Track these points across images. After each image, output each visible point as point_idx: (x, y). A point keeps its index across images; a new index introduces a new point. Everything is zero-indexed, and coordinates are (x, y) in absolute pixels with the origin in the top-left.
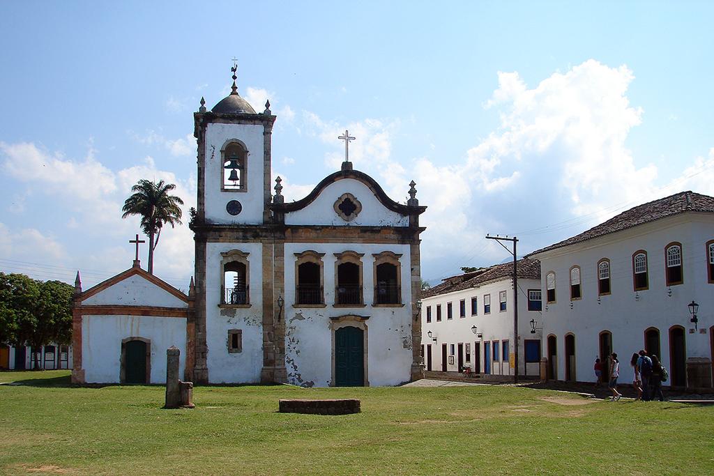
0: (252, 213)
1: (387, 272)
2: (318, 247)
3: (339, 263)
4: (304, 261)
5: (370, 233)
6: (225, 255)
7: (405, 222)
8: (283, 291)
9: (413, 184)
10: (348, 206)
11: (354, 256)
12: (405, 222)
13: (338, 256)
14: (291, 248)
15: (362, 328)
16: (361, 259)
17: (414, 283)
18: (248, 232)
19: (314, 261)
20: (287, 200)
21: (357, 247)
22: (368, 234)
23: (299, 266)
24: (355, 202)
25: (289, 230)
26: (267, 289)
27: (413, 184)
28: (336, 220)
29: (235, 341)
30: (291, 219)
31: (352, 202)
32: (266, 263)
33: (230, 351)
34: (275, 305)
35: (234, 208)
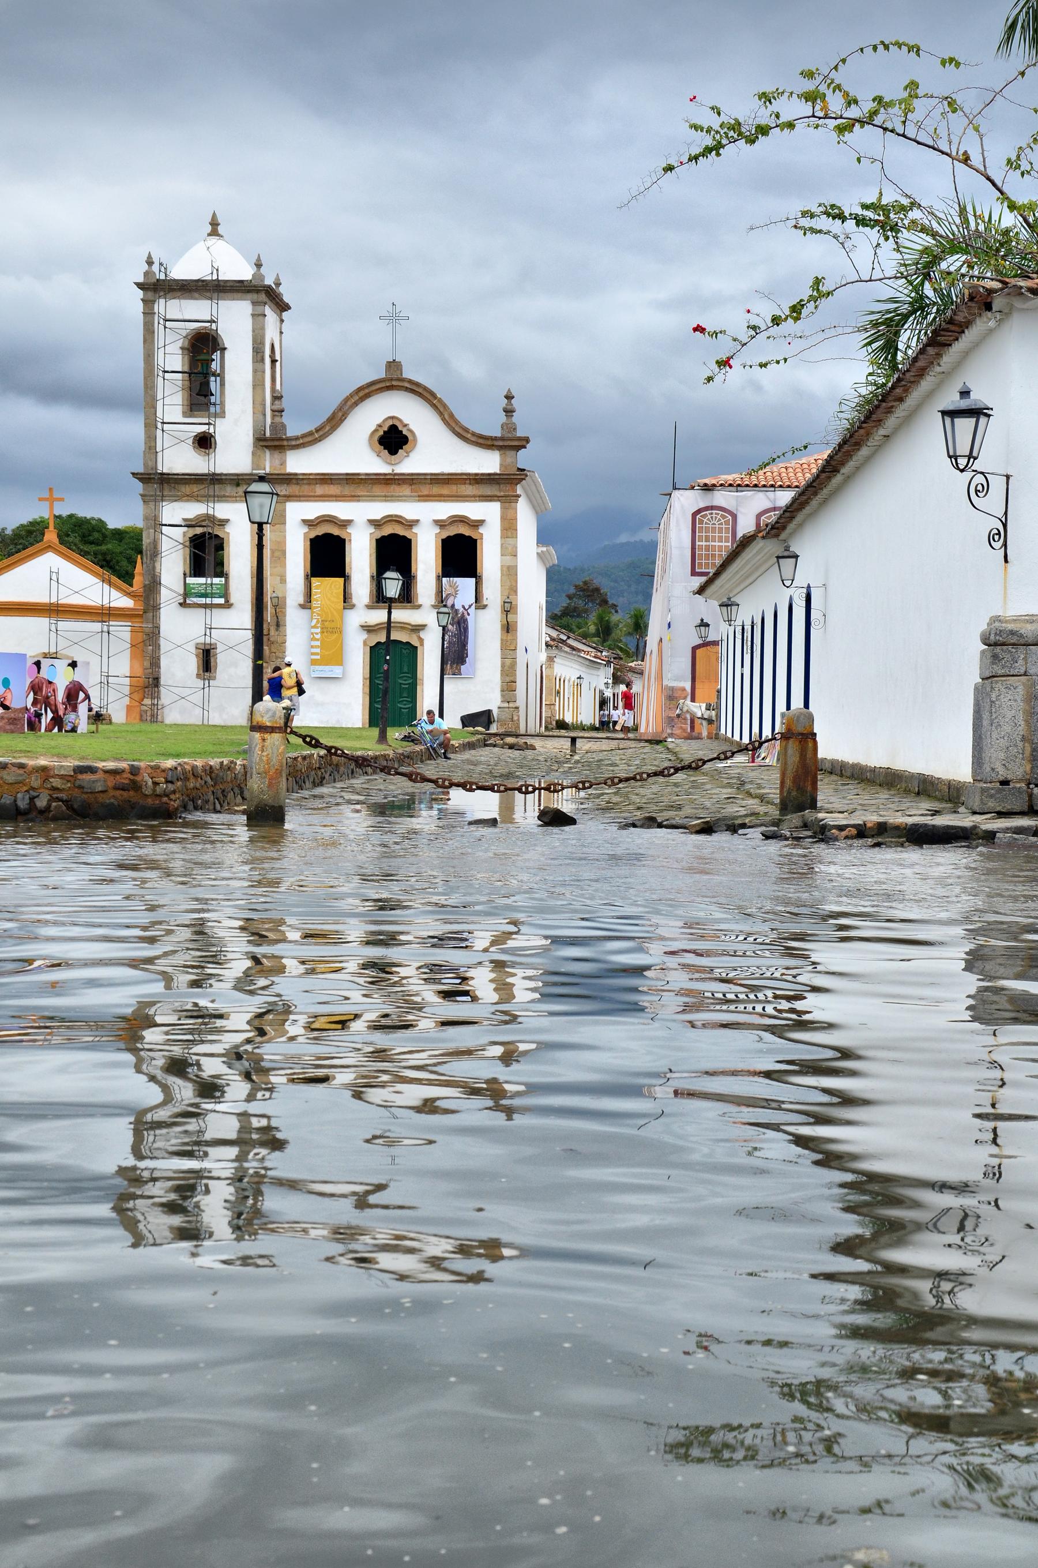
2: (340, 510)
3: (379, 534)
4: (320, 531)
8: (283, 580)
9: (509, 397)
11: (402, 523)
12: (489, 463)
13: (375, 523)
15: (415, 642)
16: (415, 530)
17: (505, 569)
19: (335, 531)
20: (290, 433)
21: (407, 510)
22: (425, 490)
23: (311, 540)
24: (405, 432)
25: (294, 481)
27: (509, 397)
28: (374, 463)
29: (207, 659)
30: (298, 463)
31: (401, 432)
33: (198, 676)
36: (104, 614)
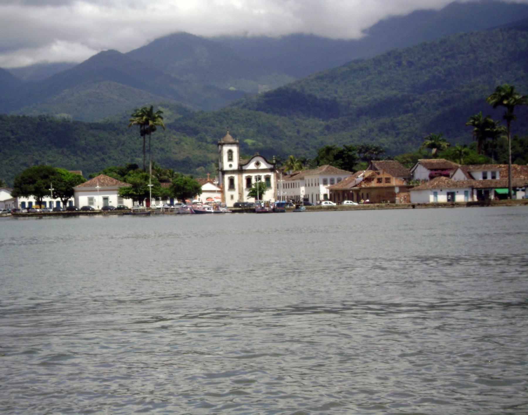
0: (235, 166)
1: (268, 179)
5: (264, 171)
6: (229, 177)
7: (272, 166)
8: (242, 185)
10: (258, 164)
12: (272, 166)
14: (245, 175)
18: (233, 172)
21: (261, 174)
26: (239, 185)
29: (232, 197)
30: (244, 168)
32: (239, 179)
34: (241, 189)
35: (231, 166)
36: (218, 191)
